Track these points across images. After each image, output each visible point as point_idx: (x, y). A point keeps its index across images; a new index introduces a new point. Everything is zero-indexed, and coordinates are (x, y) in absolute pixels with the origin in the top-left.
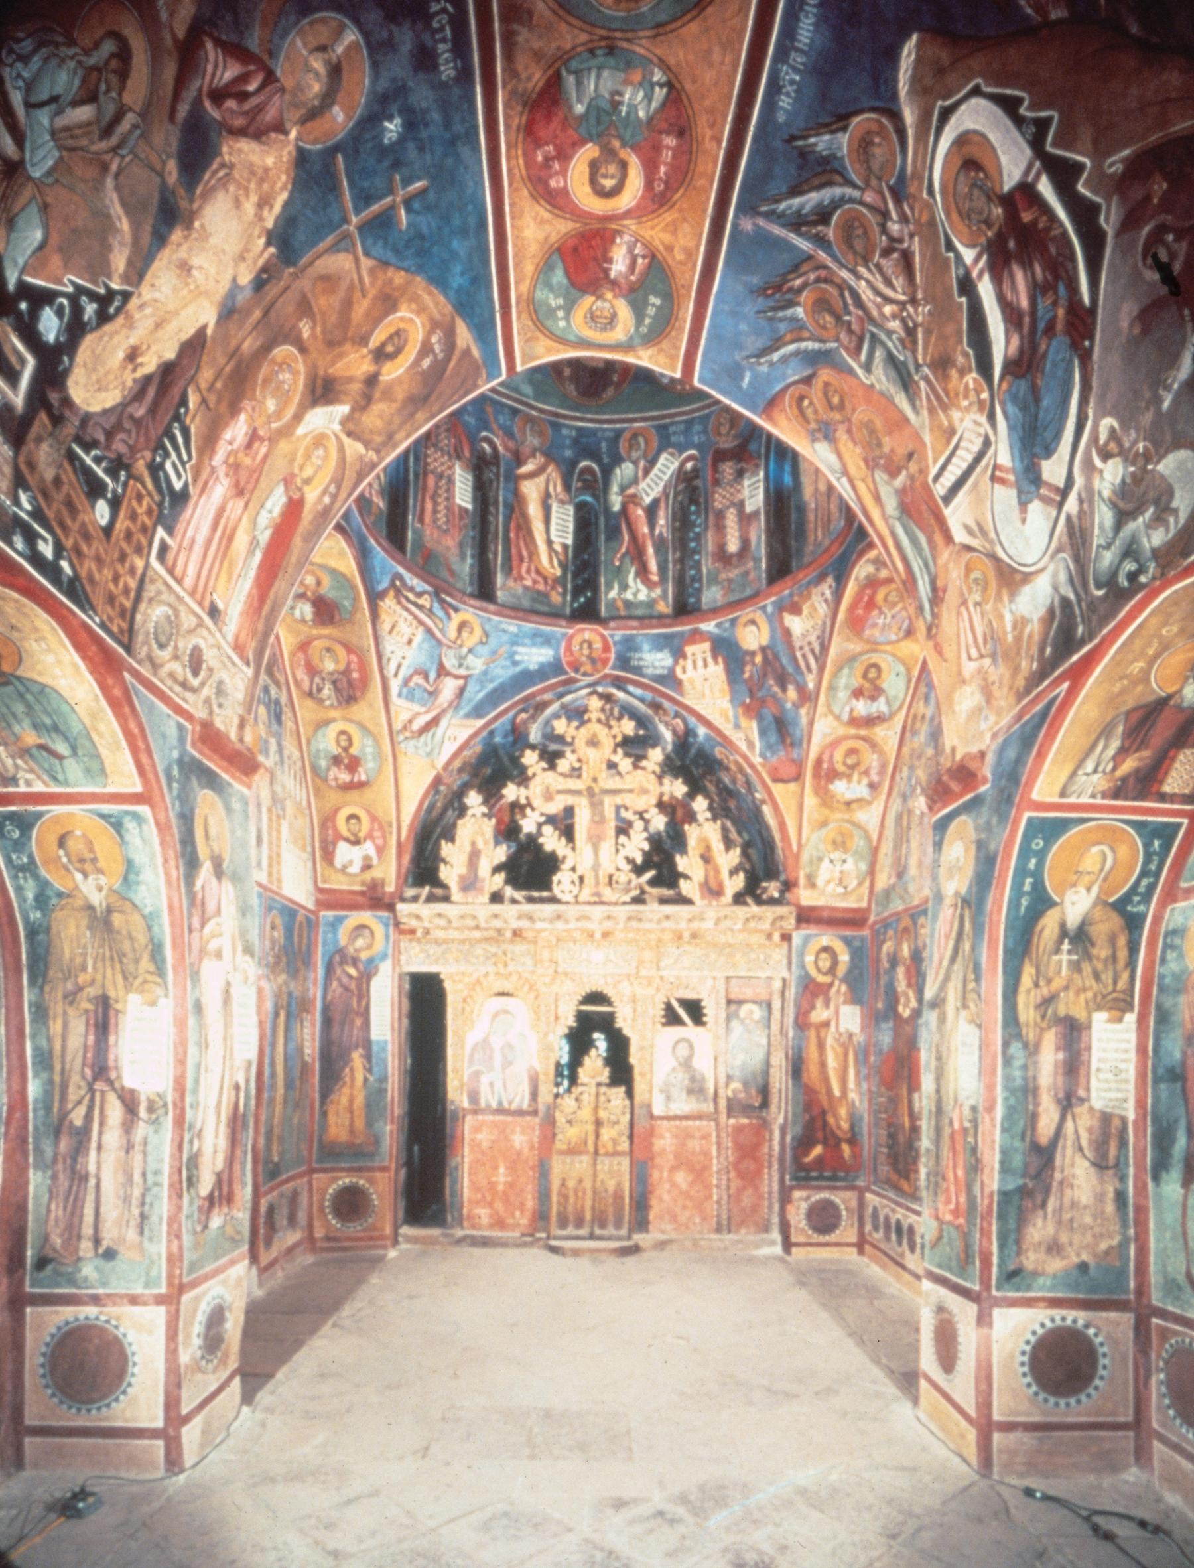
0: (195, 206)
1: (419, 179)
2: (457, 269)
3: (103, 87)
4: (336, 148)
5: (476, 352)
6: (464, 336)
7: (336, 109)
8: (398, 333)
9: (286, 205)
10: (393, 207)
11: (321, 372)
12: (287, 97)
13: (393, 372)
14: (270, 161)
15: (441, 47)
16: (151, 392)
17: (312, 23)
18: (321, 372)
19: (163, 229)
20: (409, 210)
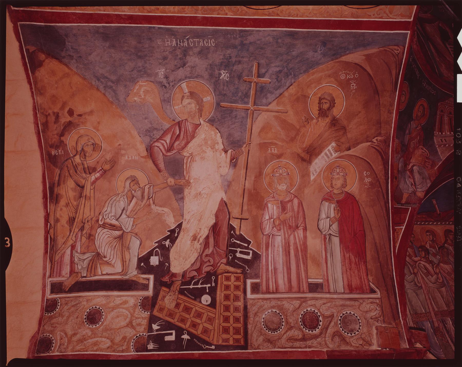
0: (187, 178)
1: (252, 66)
2: (311, 54)
3: (133, 192)
4: (218, 104)
5: (373, 50)
6: (356, 57)
7: (205, 100)
8: (320, 99)
9: (222, 137)
10: (257, 83)
11: (300, 151)
12: (189, 119)
13: (338, 111)
14: (203, 136)
15: (201, 44)
16: (211, 240)
17: (173, 100)
18: (300, 151)
19: (180, 196)
20: (263, 76)
